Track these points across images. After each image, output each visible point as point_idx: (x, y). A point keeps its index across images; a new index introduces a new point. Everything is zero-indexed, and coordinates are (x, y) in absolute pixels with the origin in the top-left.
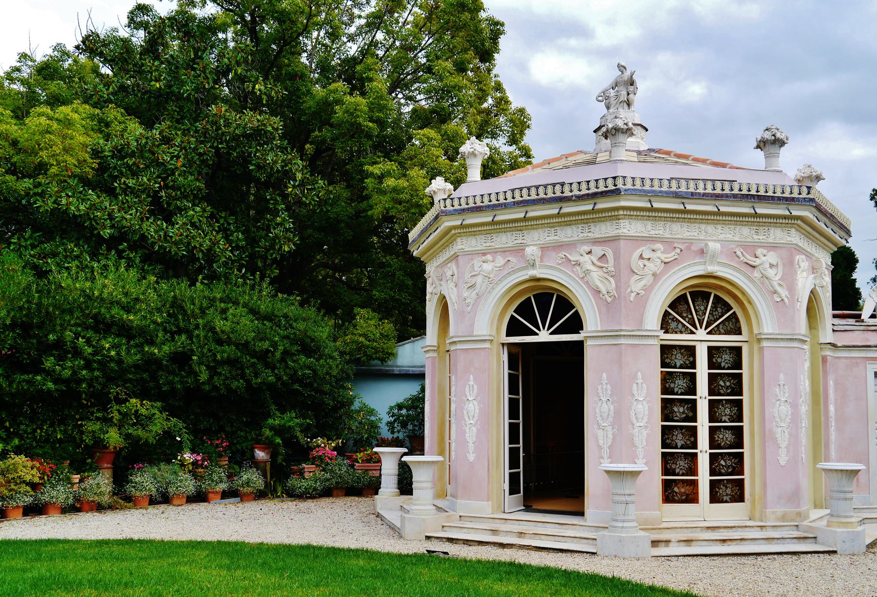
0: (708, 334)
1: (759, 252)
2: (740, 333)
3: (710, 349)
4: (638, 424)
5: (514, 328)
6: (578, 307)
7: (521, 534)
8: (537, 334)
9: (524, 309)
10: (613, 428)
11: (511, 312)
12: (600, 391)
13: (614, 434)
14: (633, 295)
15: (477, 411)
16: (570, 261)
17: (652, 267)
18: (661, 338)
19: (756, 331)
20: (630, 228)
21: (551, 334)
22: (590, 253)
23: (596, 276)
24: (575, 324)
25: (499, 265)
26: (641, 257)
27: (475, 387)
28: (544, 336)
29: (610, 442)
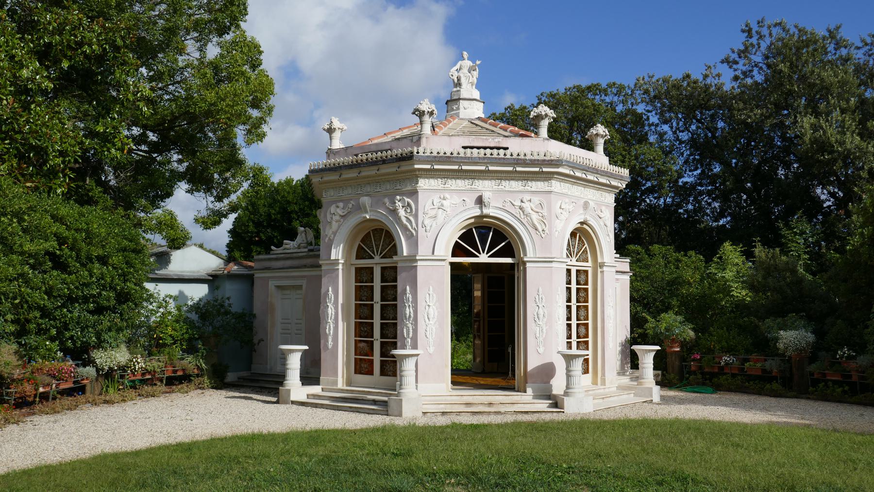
0: (489, 257)
1: (603, 208)
2: (587, 262)
3: (578, 271)
4: (559, 323)
5: (458, 250)
6: (509, 239)
7: (490, 404)
8: (478, 257)
9: (467, 236)
10: (546, 326)
11: (456, 238)
12: (537, 300)
13: (546, 330)
14: (557, 233)
15: (436, 314)
16: (513, 205)
17: (565, 214)
18: (567, 264)
19: (599, 260)
20: (556, 185)
21: (489, 257)
22: (530, 201)
23: (535, 216)
24: (508, 251)
25: (455, 203)
26: (560, 208)
27: (434, 295)
28: (484, 258)
29: (544, 336)
